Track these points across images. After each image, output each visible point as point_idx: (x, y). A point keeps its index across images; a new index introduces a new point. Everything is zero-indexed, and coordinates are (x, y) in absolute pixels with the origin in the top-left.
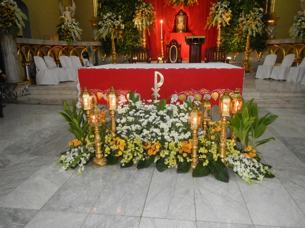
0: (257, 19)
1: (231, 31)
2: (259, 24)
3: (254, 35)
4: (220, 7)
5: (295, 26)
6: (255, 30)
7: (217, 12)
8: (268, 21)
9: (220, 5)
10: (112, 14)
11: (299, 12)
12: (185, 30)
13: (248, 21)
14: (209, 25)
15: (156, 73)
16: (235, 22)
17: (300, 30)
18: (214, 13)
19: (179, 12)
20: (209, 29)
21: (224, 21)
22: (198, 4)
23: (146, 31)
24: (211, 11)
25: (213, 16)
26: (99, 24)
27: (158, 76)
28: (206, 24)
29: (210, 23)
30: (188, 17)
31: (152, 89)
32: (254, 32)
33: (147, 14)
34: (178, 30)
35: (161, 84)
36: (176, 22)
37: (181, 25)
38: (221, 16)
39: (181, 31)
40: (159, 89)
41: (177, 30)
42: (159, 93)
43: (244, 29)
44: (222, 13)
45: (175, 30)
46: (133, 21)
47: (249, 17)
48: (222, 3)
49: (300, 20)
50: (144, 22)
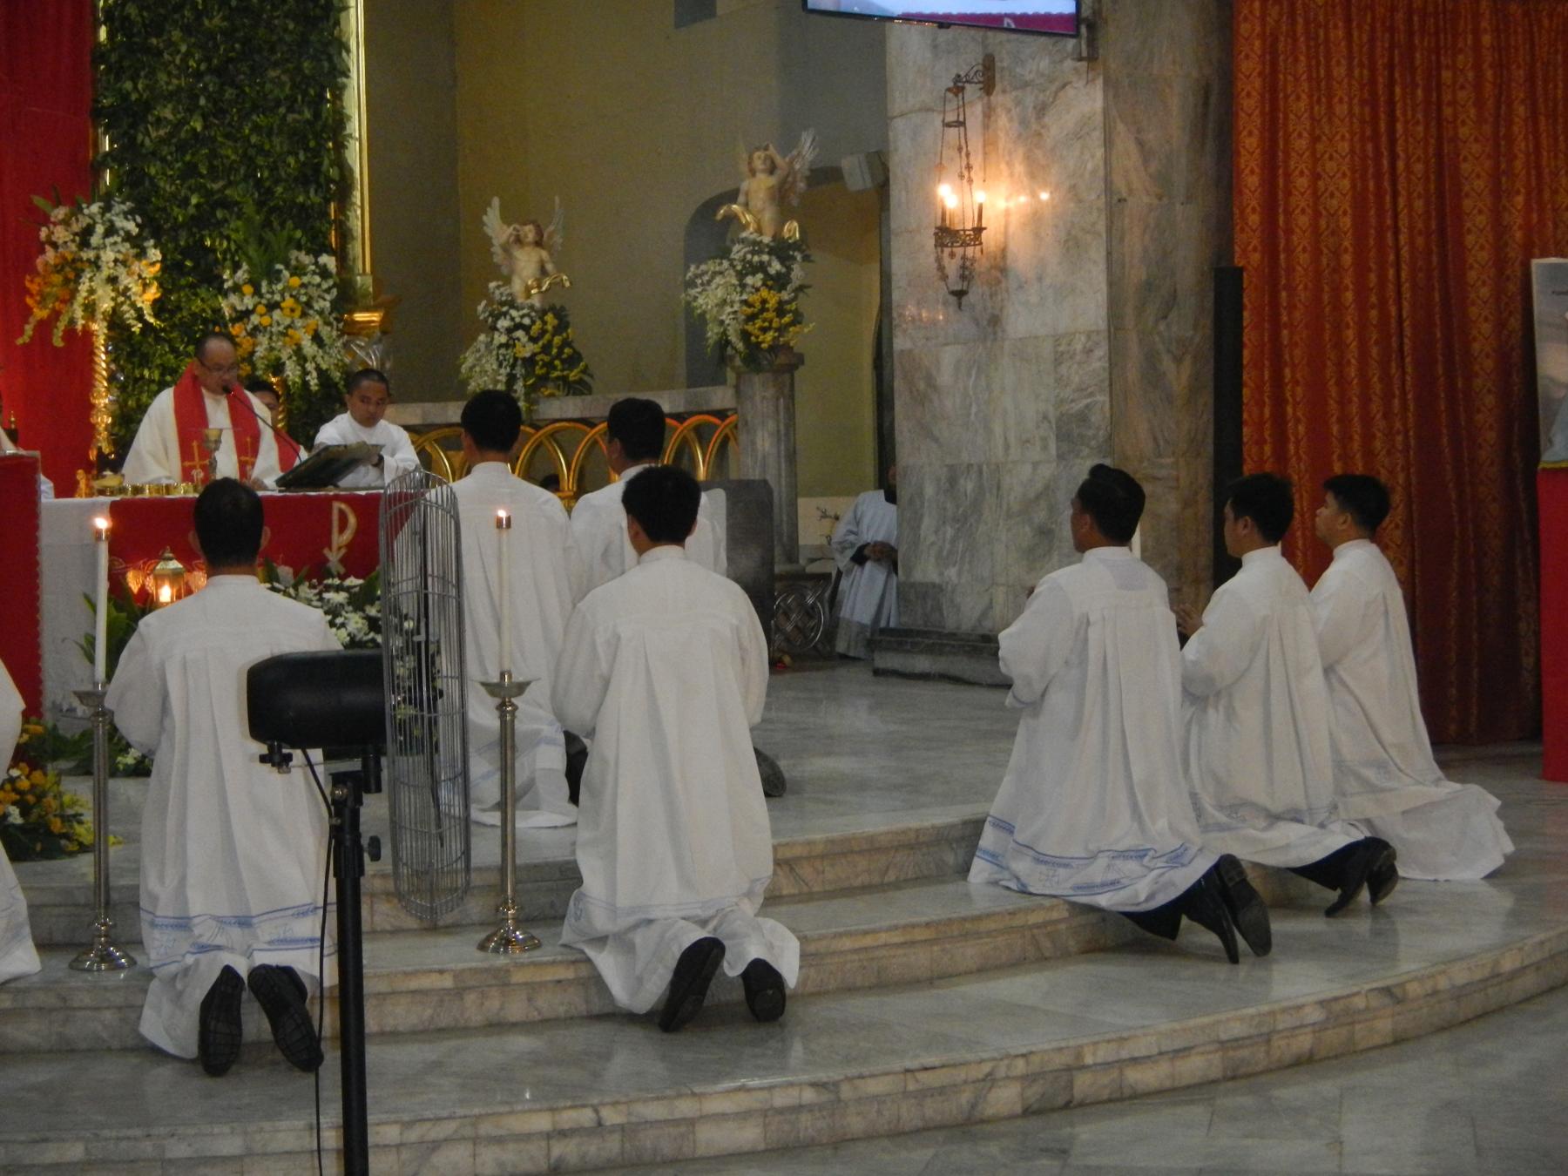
0: (316, 307)
1: (161, 356)
2: (325, 332)
3: (313, 381)
4: (100, 229)
5: (488, 345)
6: (314, 357)
7: (88, 254)
8: (351, 312)
9: (98, 219)
11: (492, 285)
13: (277, 314)
14: (45, 327)
15: (337, 505)
16: (179, 308)
17: (513, 367)
18: (70, 258)
20: (58, 342)
21: (133, 305)
24: (47, 247)
25: (72, 275)
27: (342, 512)
28: (28, 311)
29: (56, 315)
31: (326, 551)
32: (310, 366)
35: (347, 536)
38: (113, 280)
40: (343, 551)
42: (343, 561)
43: (260, 351)
44: (116, 261)
47: (277, 297)
48: (107, 208)
49: (503, 323)
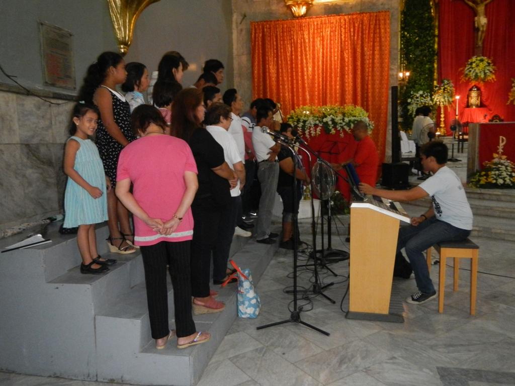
10: (424, 92)
12: (479, 104)
19: (472, 87)
22: (495, 80)
23: (445, 107)
26: (409, 100)
28: (508, 99)
30: (481, 92)
33: (449, 90)
34: (472, 105)
36: (469, 96)
37: (474, 99)
39: (474, 107)
41: (470, 104)
45: (468, 106)
46: (433, 97)
50: (446, 98)
